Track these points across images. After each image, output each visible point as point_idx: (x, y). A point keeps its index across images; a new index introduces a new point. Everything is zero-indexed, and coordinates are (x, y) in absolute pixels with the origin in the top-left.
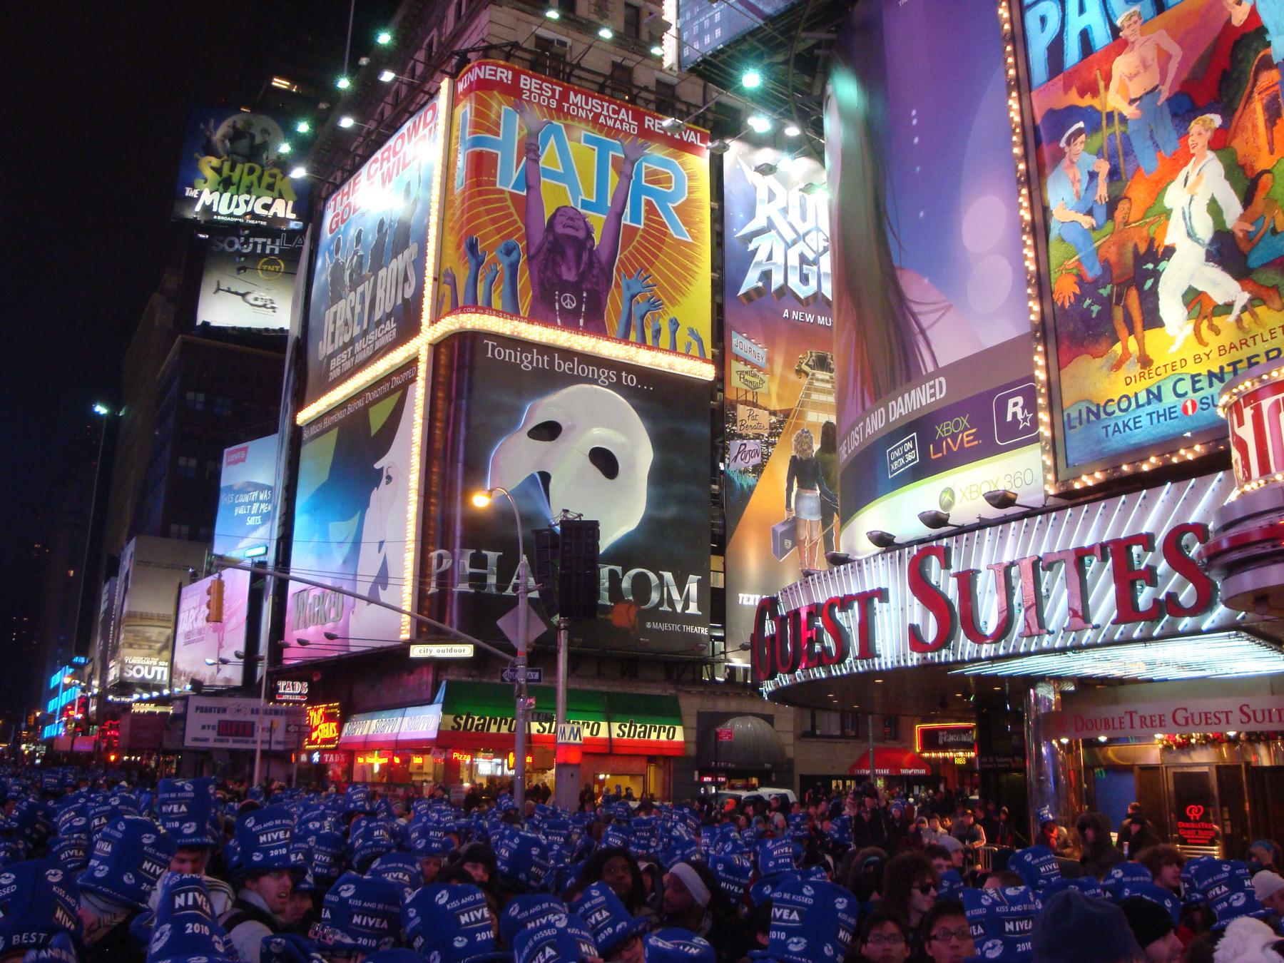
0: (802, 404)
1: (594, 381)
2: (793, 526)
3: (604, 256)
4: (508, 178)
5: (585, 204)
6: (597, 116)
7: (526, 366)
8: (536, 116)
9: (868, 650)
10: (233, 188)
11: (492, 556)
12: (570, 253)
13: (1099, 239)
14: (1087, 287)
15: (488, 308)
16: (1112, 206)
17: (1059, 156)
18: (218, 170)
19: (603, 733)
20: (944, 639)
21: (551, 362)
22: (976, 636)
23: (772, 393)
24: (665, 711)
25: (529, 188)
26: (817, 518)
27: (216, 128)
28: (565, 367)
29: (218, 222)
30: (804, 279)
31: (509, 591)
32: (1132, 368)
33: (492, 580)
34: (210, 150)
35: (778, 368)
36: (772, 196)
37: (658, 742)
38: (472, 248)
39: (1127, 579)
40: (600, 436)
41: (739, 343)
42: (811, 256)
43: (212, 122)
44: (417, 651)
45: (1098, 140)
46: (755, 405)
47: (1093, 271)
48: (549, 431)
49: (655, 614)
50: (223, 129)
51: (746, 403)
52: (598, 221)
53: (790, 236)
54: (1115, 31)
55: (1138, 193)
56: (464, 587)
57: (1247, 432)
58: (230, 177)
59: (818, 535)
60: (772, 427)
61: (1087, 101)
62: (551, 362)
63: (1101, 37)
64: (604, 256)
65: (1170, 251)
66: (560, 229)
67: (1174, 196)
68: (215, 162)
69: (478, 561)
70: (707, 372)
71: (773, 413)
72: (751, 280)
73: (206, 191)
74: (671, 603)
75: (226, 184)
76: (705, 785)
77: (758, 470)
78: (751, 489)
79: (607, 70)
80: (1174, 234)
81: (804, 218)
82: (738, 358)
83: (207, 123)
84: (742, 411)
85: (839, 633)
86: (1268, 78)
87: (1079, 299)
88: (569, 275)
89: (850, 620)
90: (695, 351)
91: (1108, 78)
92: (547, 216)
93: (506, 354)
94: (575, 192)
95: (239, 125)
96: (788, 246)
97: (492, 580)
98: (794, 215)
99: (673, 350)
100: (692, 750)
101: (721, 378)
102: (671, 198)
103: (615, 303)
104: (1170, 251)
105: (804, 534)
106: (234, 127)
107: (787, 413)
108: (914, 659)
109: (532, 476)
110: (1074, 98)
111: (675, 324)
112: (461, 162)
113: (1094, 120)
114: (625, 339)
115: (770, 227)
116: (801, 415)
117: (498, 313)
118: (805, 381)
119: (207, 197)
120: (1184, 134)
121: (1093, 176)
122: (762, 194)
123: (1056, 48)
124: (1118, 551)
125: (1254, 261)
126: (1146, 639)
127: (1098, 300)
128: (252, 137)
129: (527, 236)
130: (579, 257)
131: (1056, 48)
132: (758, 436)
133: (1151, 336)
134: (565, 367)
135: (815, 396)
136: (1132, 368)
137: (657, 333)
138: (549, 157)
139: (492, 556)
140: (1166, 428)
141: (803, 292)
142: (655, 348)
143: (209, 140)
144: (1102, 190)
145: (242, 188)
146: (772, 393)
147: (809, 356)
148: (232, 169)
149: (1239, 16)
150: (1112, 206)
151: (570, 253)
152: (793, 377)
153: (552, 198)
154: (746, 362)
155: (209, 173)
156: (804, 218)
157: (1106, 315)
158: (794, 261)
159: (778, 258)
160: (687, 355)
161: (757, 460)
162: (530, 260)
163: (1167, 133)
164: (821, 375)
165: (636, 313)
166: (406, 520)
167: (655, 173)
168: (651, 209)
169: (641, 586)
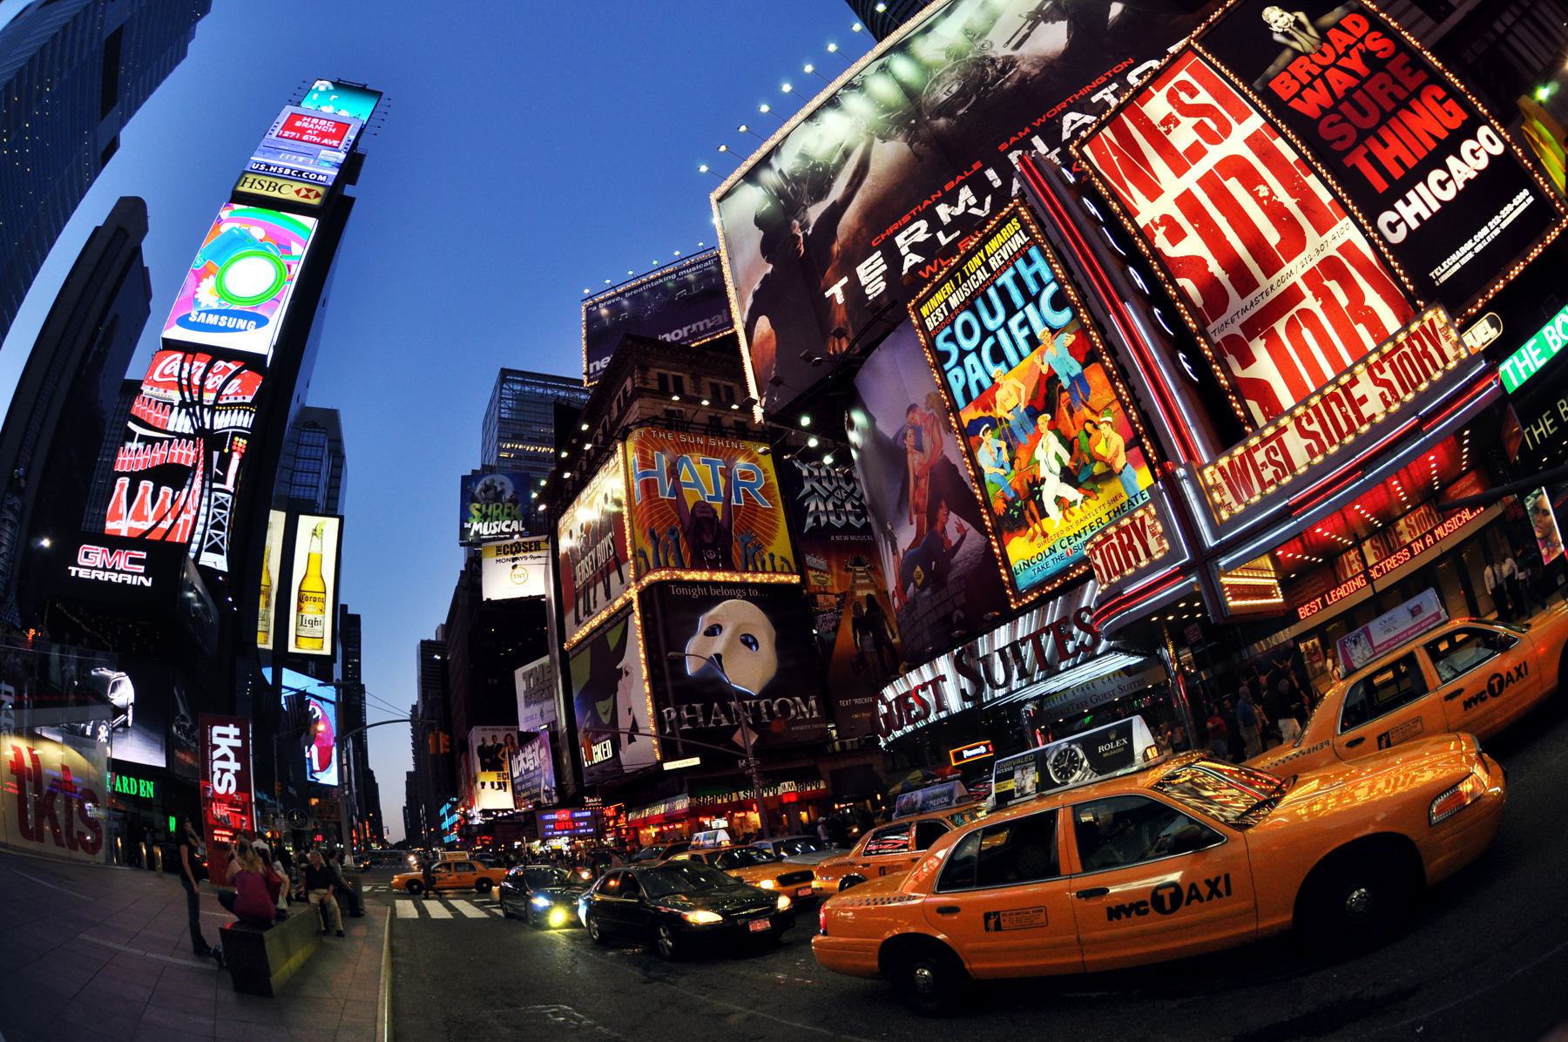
1: (734, 597)
4: (665, 492)
5: (710, 498)
7: (695, 595)
8: (671, 452)
9: (940, 707)
13: (1010, 479)
14: (1010, 504)
18: (479, 510)
22: (995, 686)
32: (1040, 539)
35: (835, 570)
38: (652, 534)
41: (811, 560)
44: (668, 766)
45: (997, 432)
46: (826, 593)
48: (713, 631)
49: (795, 722)
50: (480, 487)
52: (718, 505)
54: (992, 380)
55: (1022, 454)
57: (1099, 561)
61: (987, 414)
63: (987, 384)
66: (698, 515)
67: (1039, 454)
70: (796, 579)
74: (803, 714)
75: (485, 517)
77: (836, 629)
78: (834, 641)
79: (707, 421)
80: (1043, 472)
84: (820, 598)
86: (1065, 396)
87: (1007, 510)
88: (708, 540)
90: (786, 569)
91: (995, 402)
93: (682, 591)
99: (774, 571)
100: (830, 792)
101: (804, 580)
103: (737, 551)
104: (1044, 480)
107: (844, 594)
111: (772, 556)
112: (637, 486)
113: (994, 423)
116: (853, 593)
119: (476, 527)
120: (1036, 424)
121: (999, 449)
123: (966, 390)
125: (1081, 479)
126: (1075, 666)
127: (1016, 509)
129: (681, 522)
131: (966, 390)
133: (1044, 521)
136: (1040, 539)
138: (685, 475)
140: (1061, 564)
144: (1005, 456)
149: (1045, 370)
153: (691, 497)
155: (475, 513)
162: (685, 535)
169: (784, 707)
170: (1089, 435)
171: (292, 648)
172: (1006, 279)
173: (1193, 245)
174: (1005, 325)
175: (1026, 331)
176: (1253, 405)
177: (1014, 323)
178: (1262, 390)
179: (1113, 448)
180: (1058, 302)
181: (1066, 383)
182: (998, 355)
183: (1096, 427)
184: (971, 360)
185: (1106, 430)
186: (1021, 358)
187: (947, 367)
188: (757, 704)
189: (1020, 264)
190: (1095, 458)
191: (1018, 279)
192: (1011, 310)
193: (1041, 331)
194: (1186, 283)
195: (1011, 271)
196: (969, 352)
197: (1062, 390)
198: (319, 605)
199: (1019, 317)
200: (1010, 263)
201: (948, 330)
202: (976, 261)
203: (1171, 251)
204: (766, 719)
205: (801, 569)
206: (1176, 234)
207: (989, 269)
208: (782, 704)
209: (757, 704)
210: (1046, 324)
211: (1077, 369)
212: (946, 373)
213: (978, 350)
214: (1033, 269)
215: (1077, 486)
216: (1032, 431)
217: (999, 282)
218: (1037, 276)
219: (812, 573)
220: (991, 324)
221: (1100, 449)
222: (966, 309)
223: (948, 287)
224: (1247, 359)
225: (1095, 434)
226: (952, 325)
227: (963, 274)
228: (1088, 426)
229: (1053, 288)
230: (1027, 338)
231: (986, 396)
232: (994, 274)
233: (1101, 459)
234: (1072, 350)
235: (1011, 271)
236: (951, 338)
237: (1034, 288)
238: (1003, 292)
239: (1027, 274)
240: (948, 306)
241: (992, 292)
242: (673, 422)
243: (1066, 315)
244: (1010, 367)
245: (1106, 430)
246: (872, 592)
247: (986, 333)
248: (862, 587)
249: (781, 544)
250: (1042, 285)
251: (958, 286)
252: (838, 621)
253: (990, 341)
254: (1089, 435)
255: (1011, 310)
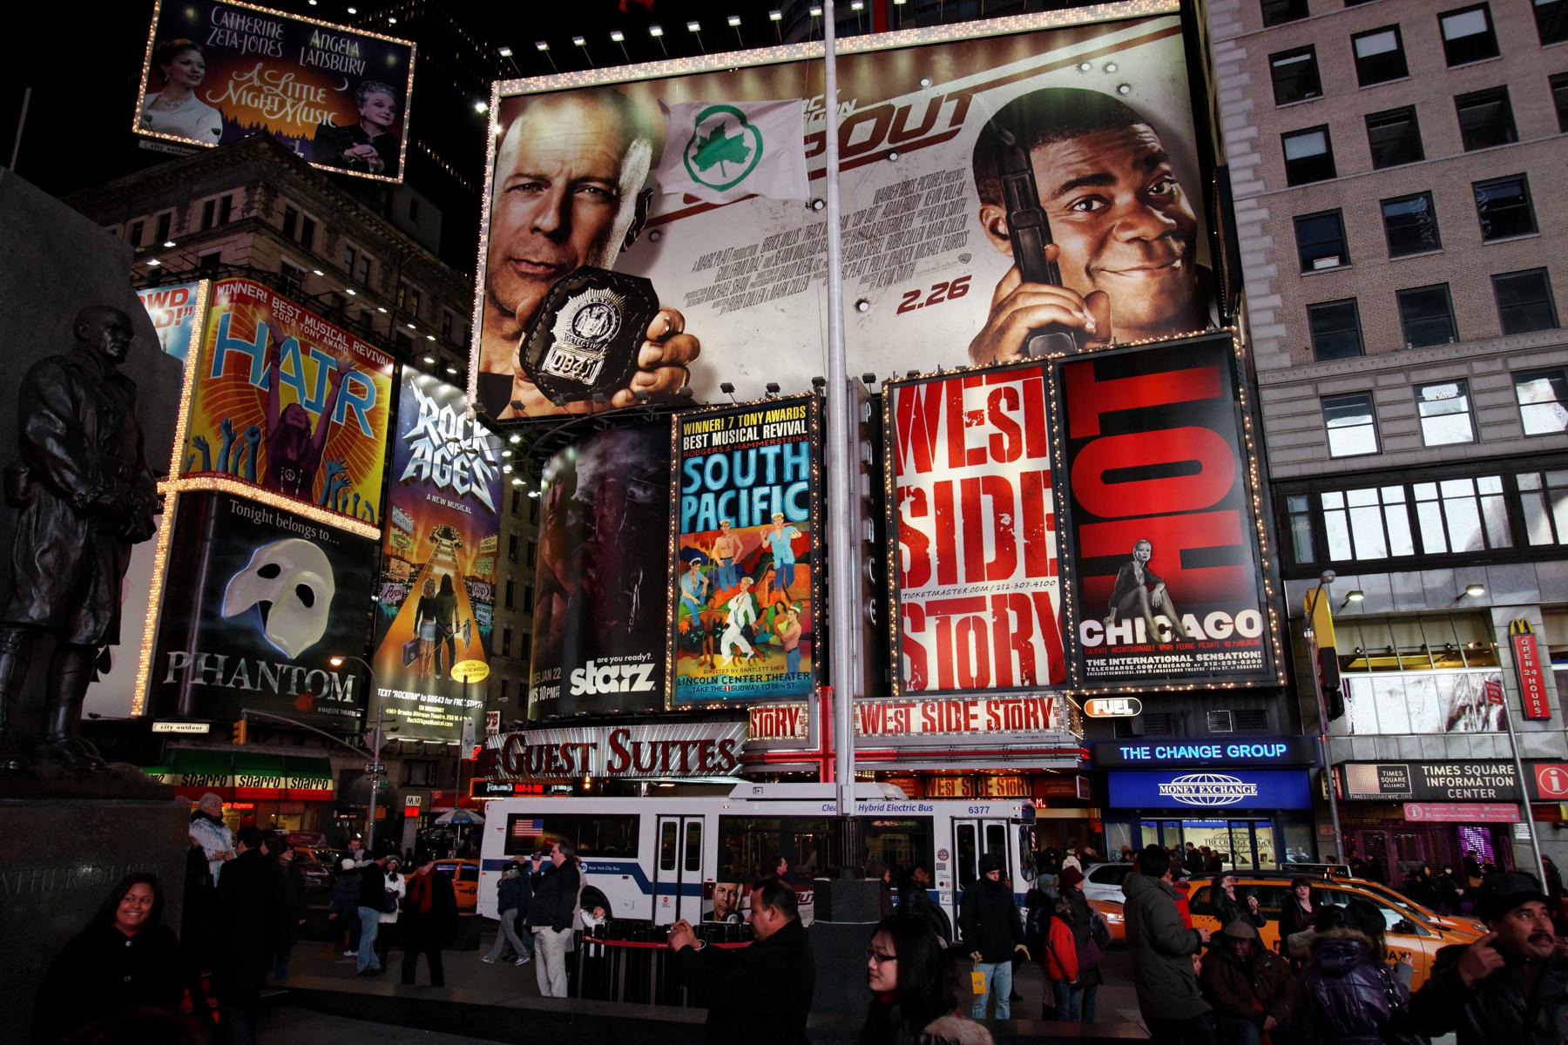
0: (432, 561)
1: (301, 536)
2: (417, 643)
3: (316, 444)
4: (258, 377)
5: (308, 404)
6: (322, 336)
11: (221, 658)
12: (294, 439)
14: (693, 629)
15: (233, 476)
16: (708, 598)
17: (688, 569)
19: (282, 786)
20: (625, 767)
21: (274, 520)
23: (414, 553)
24: (319, 769)
25: (271, 387)
26: (432, 639)
28: (283, 523)
30: (443, 474)
31: (231, 685)
33: (220, 676)
35: (419, 536)
36: (430, 411)
37: (267, 789)
39: (703, 756)
40: (308, 577)
41: (398, 515)
42: (449, 458)
45: (705, 569)
46: (402, 559)
47: (696, 623)
48: (271, 571)
49: (325, 702)
51: (396, 557)
52: (315, 416)
53: (437, 442)
54: (719, 526)
55: (719, 597)
56: (200, 681)
59: (432, 651)
60: (411, 575)
62: (274, 520)
63: (713, 526)
64: (316, 444)
65: (728, 626)
66: (289, 421)
67: (732, 604)
69: (211, 662)
70: (375, 534)
71: (413, 566)
72: (410, 470)
76: (339, 819)
77: (399, 604)
78: (394, 617)
80: (730, 620)
81: (447, 431)
82: (395, 526)
84: (394, 563)
85: (570, 761)
86: (771, 573)
87: (689, 633)
88: (292, 455)
89: (577, 755)
90: (368, 518)
92: (282, 409)
93: (245, 511)
94: (302, 394)
96: (436, 449)
97: (220, 676)
98: (442, 428)
99: (354, 517)
101: (382, 541)
102: (363, 405)
103: (320, 480)
104: (728, 626)
105: (423, 650)
107: (421, 566)
108: (607, 774)
109: (254, 607)
110: (697, 546)
111: (357, 497)
113: (706, 561)
114: (323, 507)
115: (426, 434)
116: (430, 568)
117: (241, 480)
118: (435, 545)
120: (739, 581)
122: (423, 409)
123: (694, 520)
124: (704, 745)
129: (267, 423)
130: (300, 443)
131: (694, 520)
132: (401, 581)
134: (283, 523)
135: (440, 556)
137: (345, 504)
138: (287, 364)
139: (221, 658)
141: (441, 483)
142: (342, 514)
144: (704, 591)
146: (414, 553)
147: (438, 529)
149: (765, 545)
150: (708, 598)
151: (294, 439)
152: (428, 542)
153: (287, 395)
154: (400, 529)
156: (447, 431)
157: (699, 642)
158: (438, 460)
159: (428, 457)
160: (362, 521)
161: (399, 598)
162: (267, 442)
163: (733, 577)
164: (445, 541)
165: (334, 487)
166: (144, 625)
167: (356, 385)
168: (351, 412)
170: (777, 613)
172: (771, 452)
173: (926, 525)
174: (750, 489)
175: (764, 505)
176: (907, 659)
177: (759, 492)
178: (918, 653)
179: (791, 632)
180: (802, 500)
181: (777, 564)
182: (733, 509)
183: (785, 610)
184: (708, 498)
185: (791, 616)
186: (751, 523)
187: (686, 490)
188: (289, 671)
189: (788, 448)
190: (774, 631)
191: (779, 459)
192: (761, 480)
193: (776, 513)
194: (905, 549)
195: (777, 449)
196: (708, 491)
197: (771, 568)
199: (765, 490)
200: (781, 441)
201: (699, 460)
202: (753, 418)
203: (908, 519)
204: (293, 691)
205: (384, 524)
206: (919, 509)
207: (760, 433)
208: (318, 678)
209: (289, 671)
210: (783, 511)
211: (790, 559)
212: (683, 495)
213: (718, 494)
214: (796, 460)
215: (752, 644)
216: (734, 584)
217: (763, 450)
218: (796, 468)
219: (394, 531)
220: (739, 481)
221: (782, 627)
222: (724, 453)
223: (718, 423)
224: (918, 626)
225: (782, 614)
226: (706, 458)
227: (736, 421)
228: (780, 606)
229: (803, 486)
230: (763, 511)
231: (708, 536)
232: (762, 442)
233: (778, 633)
234: (794, 543)
235: (777, 449)
236: (700, 468)
237: (788, 476)
238: (762, 460)
239: (789, 460)
240: (710, 439)
241: (752, 454)
242: (284, 284)
243: (801, 515)
244: (738, 525)
245: (791, 616)
246: (451, 573)
247: (730, 485)
248: (443, 564)
249: (371, 487)
250: (796, 479)
251: (726, 428)
252: (405, 596)
253: (730, 494)
254: (777, 613)
255: (761, 480)
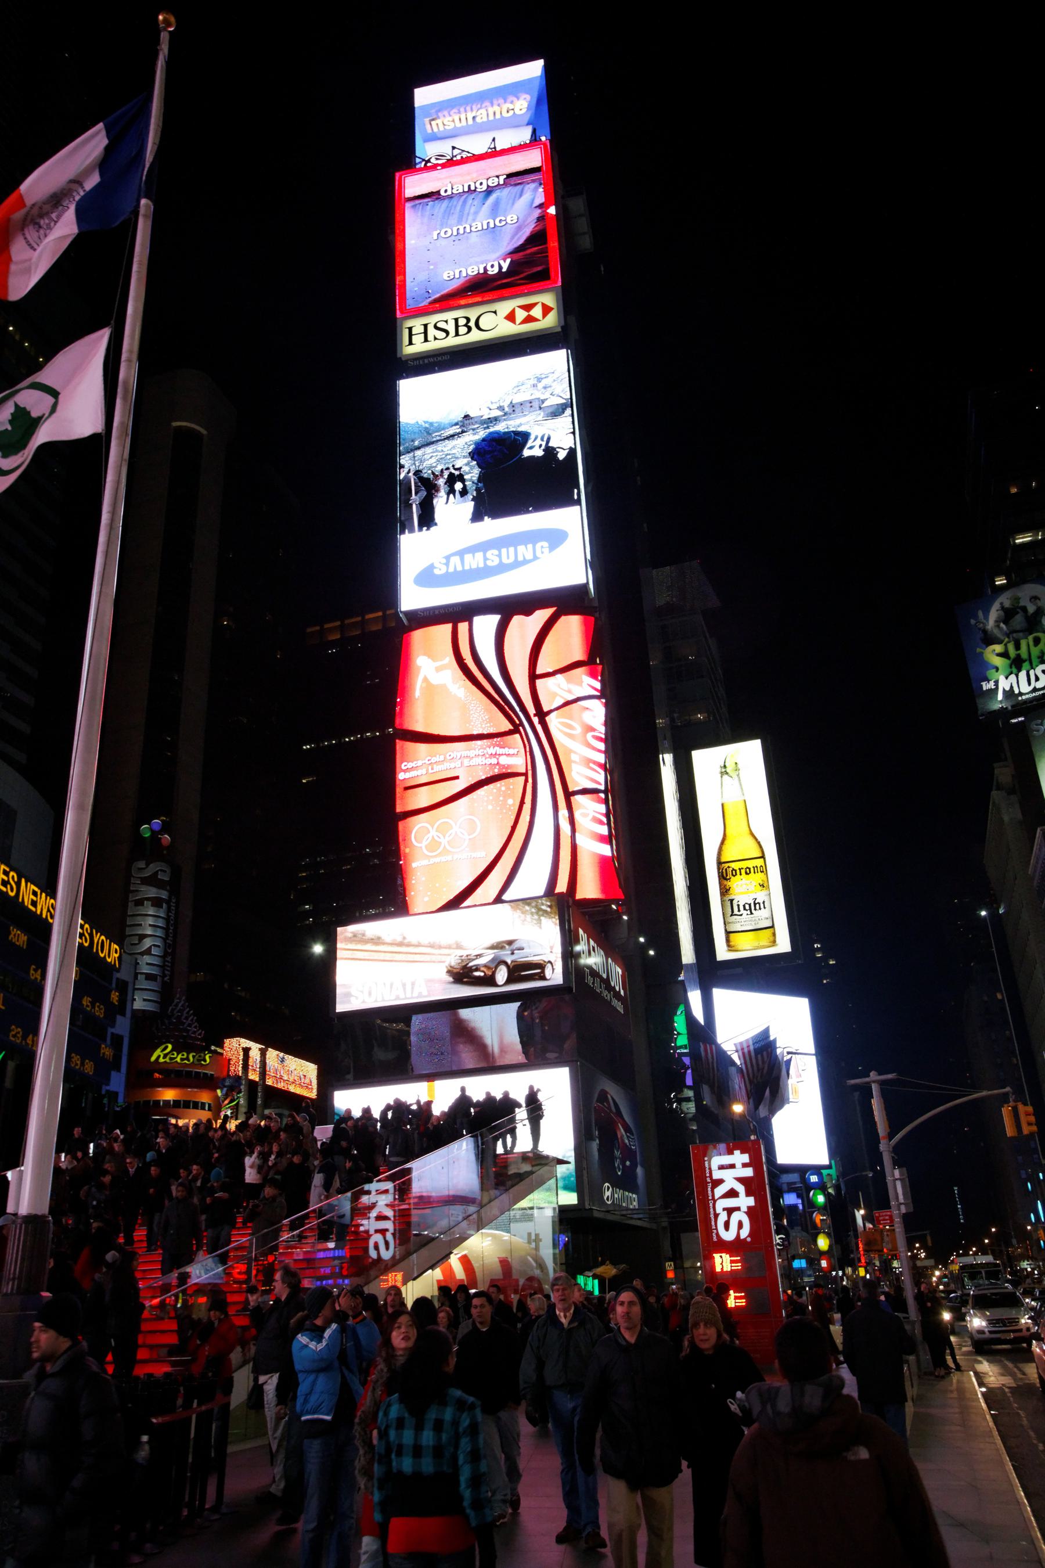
10: (1026, 665)
18: (1004, 655)
27: (986, 617)
29: (1025, 702)
34: (989, 640)
43: (980, 614)
50: (994, 614)
58: (1018, 656)
68: (998, 648)
73: (1002, 679)
75: (1016, 664)
83: (976, 617)
95: (1007, 604)
106: (1003, 608)
119: (1004, 684)
128: (1024, 609)
143: (985, 631)
145: (1035, 661)
148: (1018, 647)
155: (998, 661)
171: (722, 954)
198: (759, 877)
